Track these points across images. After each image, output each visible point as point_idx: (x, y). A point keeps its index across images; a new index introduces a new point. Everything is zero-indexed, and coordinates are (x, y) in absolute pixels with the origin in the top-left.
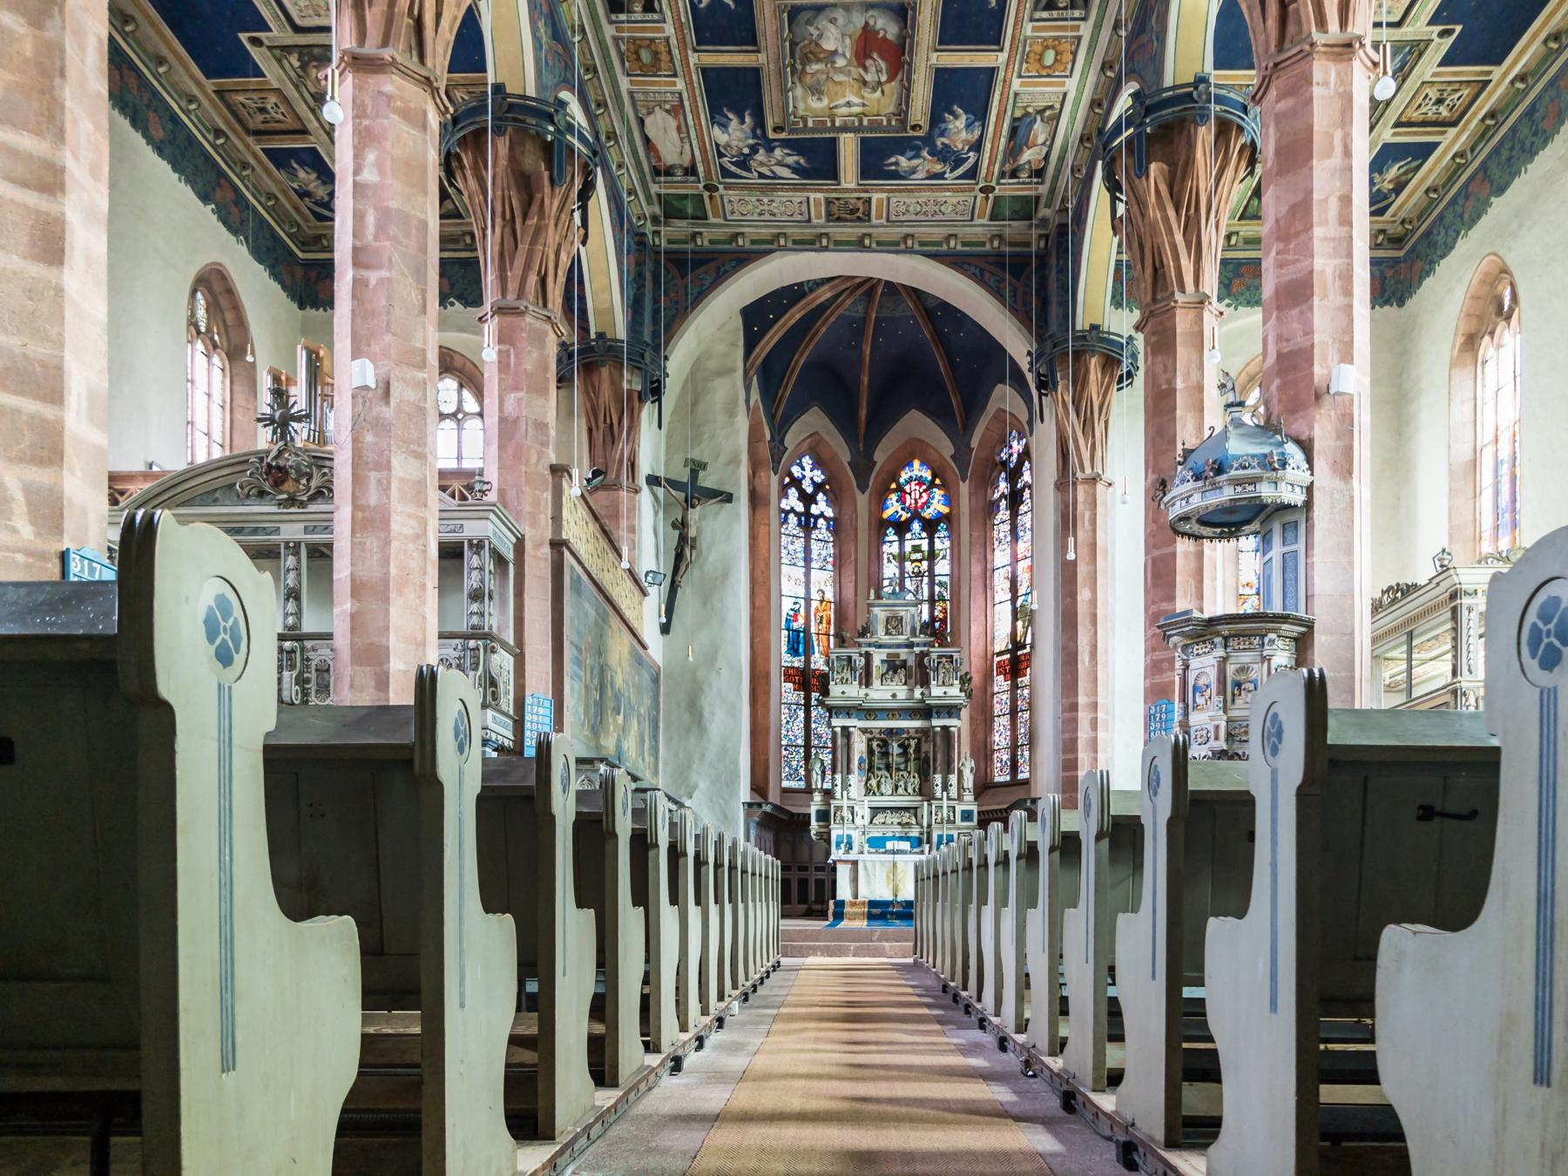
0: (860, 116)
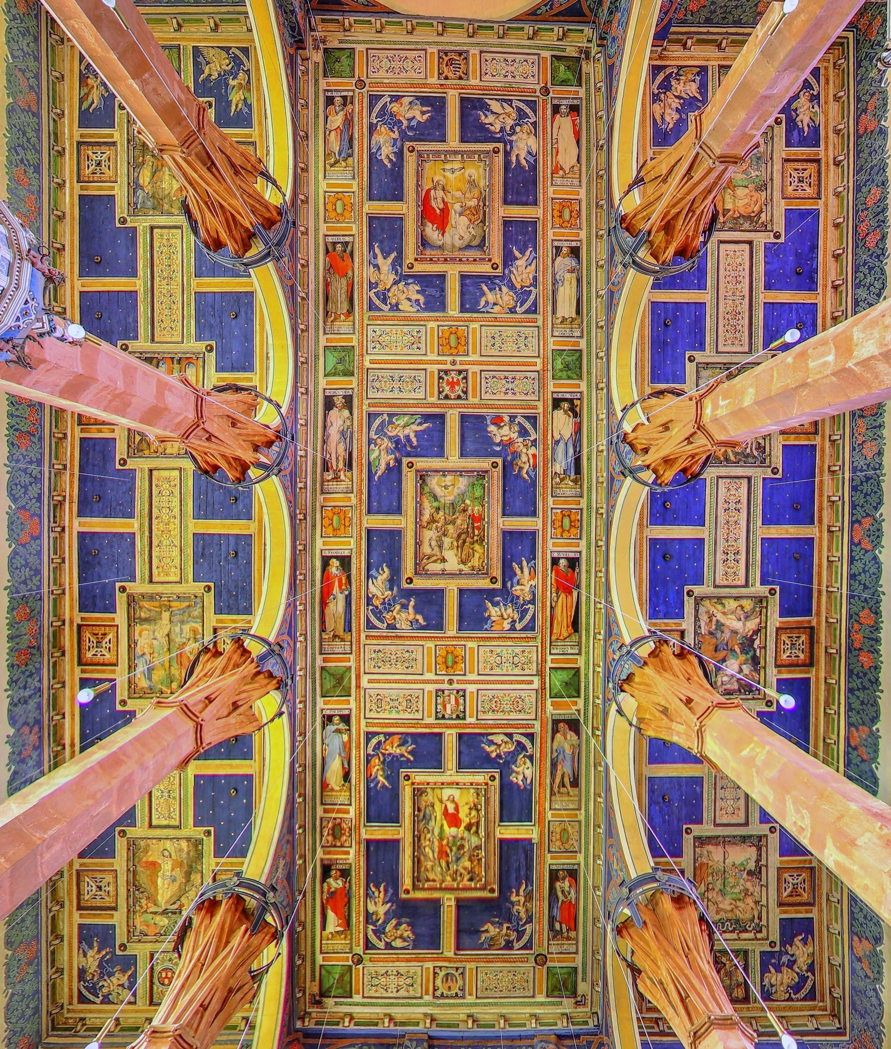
0: (445, 162)
